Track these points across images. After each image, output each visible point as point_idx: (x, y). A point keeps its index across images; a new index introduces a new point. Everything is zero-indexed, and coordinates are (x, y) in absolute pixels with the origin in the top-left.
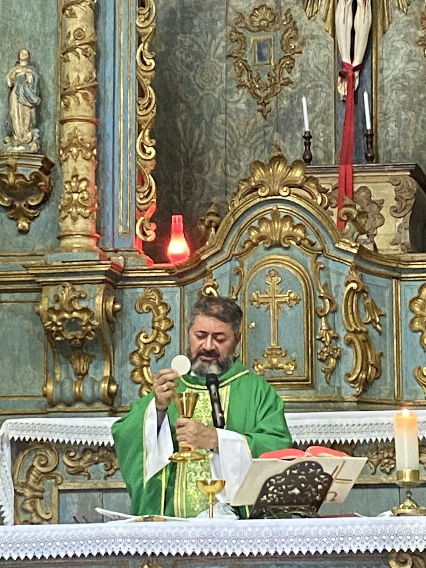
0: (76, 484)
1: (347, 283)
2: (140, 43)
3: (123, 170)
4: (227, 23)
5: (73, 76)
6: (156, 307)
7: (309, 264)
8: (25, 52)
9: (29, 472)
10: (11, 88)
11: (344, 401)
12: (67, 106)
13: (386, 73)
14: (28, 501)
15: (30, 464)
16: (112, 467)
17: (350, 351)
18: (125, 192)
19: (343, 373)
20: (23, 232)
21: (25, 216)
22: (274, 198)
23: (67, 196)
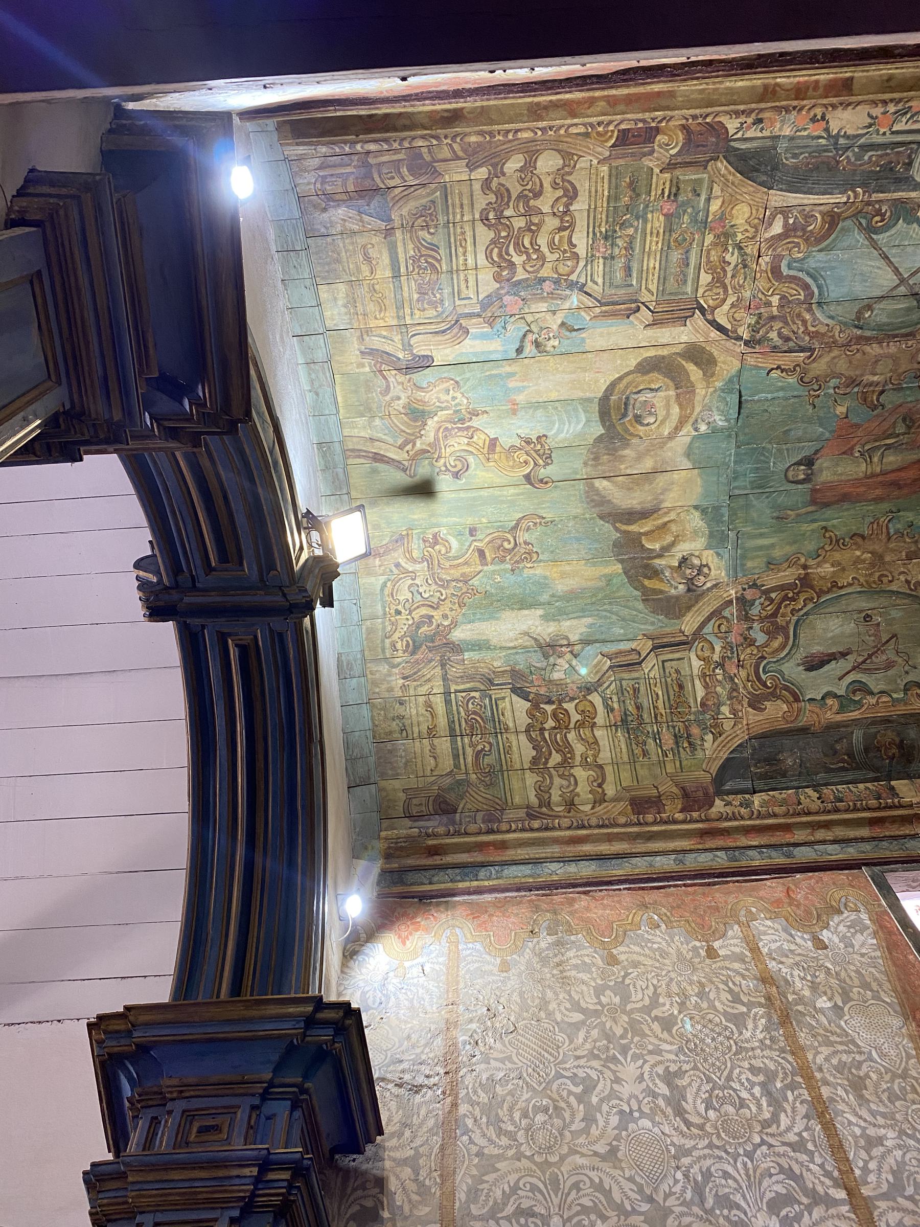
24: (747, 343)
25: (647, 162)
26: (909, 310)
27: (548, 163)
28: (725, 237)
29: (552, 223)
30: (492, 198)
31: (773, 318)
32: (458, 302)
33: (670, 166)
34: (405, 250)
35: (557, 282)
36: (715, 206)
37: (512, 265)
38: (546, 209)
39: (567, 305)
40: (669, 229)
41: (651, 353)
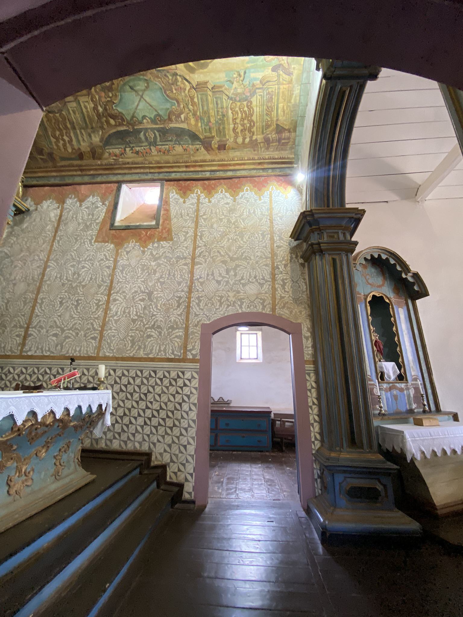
24: (177, 74)
25: (217, 139)
26: (135, 86)
27: (240, 140)
28: (194, 115)
29: (238, 121)
30: (252, 130)
31: (173, 84)
32: (262, 94)
33: (213, 137)
34: (274, 114)
35: (235, 100)
36: (200, 124)
37: (247, 106)
38: (239, 125)
39: (232, 91)
40: (209, 117)
41: (205, 70)
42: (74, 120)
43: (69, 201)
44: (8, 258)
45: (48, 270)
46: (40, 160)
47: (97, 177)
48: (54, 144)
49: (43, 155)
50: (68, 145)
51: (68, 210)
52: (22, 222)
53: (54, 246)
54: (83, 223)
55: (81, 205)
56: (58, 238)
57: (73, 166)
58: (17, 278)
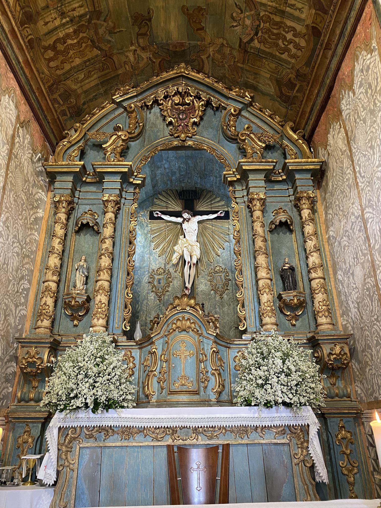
0: (89, 444)
1: (212, 348)
2: (129, 257)
3: (119, 303)
4: (149, 272)
5: (103, 264)
6: (129, 358)
7: (197, 340)
8: (84, 257)
9: (66, 437)
10: (77, 270)
11: (211, 401)
12: (99, 275)
13: (198, 289)
14: (64, 454)
15: (67, 433)
16: (108, 434)
17: (213, 378)
18: (119, 311)
19: (211, 388)
20: (76, 326)
21: (77, 320)
22: (183, 311)
23: (96, 310)
42: (274, 4)
43: (344, 105)
44: (335, 242)
45: (368, 226)
46: (298, 94)
47: (346, 30)
48: (289, 59)
49: (296, 85)
50: (297, 40)
51: (347, 117)
52: (327, 185)
53: (360, 184)
54: (367, 114)
55: (354, 94)
56: (358, 169)
57: (318, 56)
58: (351, 263)
